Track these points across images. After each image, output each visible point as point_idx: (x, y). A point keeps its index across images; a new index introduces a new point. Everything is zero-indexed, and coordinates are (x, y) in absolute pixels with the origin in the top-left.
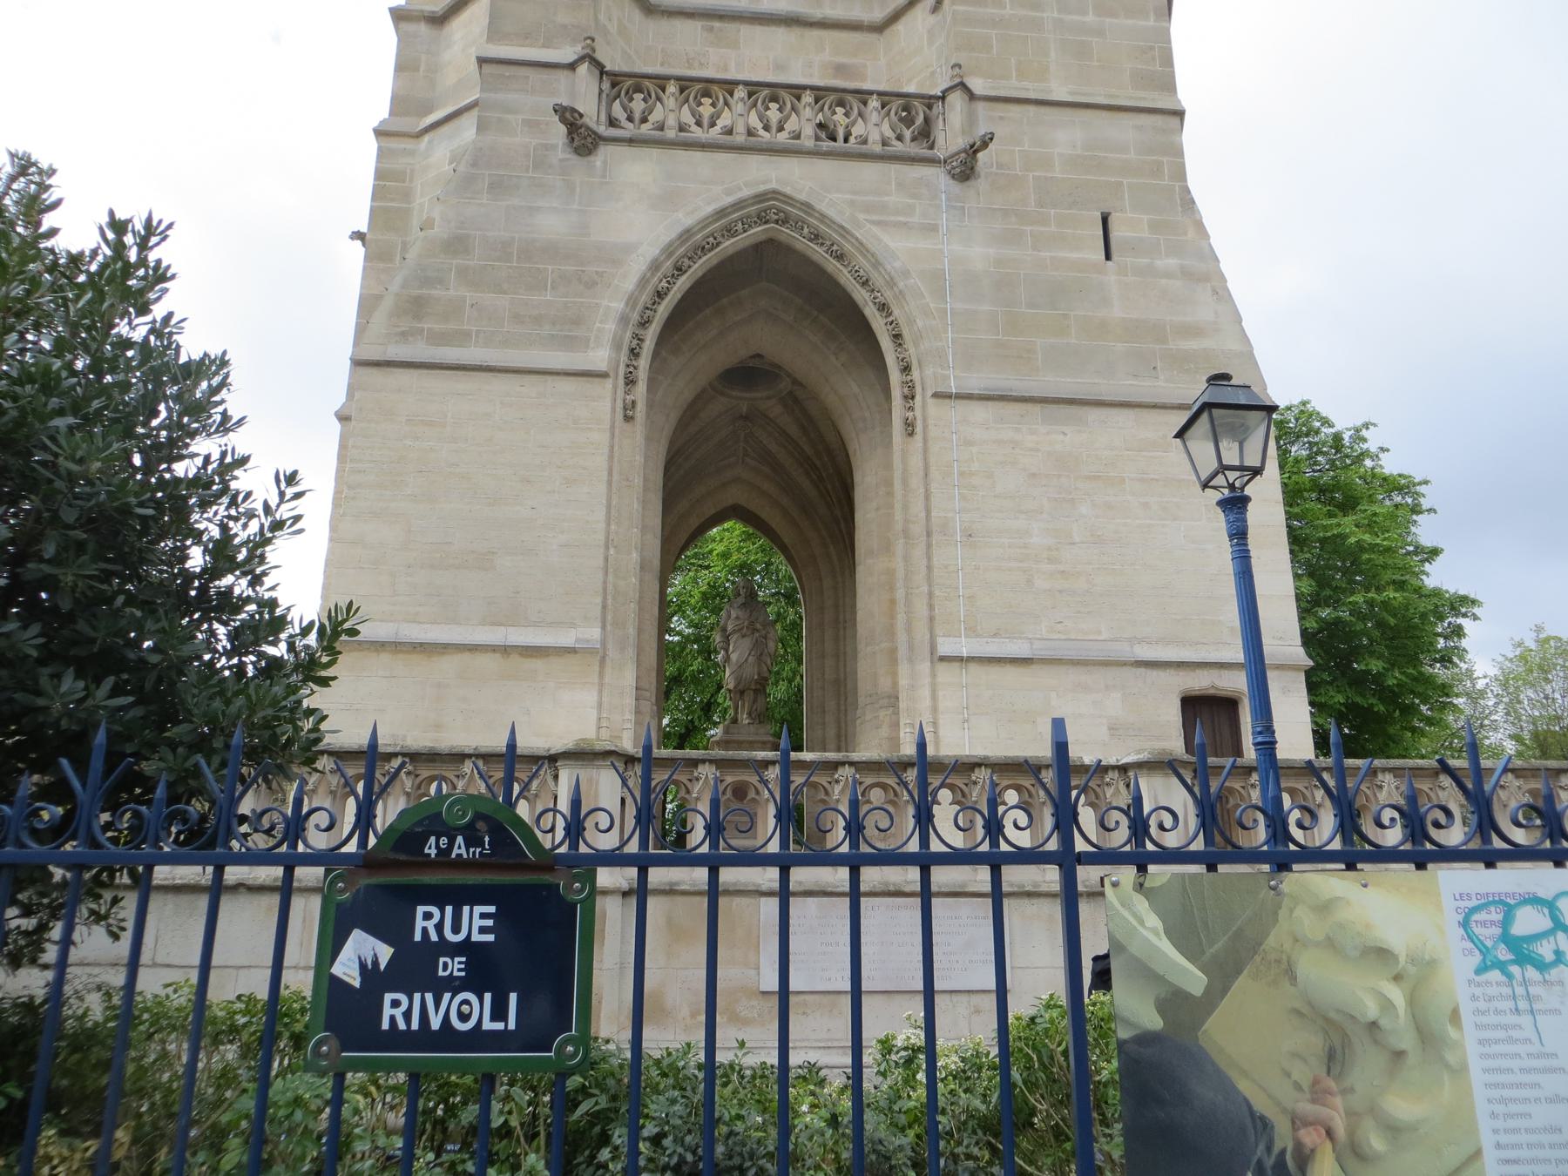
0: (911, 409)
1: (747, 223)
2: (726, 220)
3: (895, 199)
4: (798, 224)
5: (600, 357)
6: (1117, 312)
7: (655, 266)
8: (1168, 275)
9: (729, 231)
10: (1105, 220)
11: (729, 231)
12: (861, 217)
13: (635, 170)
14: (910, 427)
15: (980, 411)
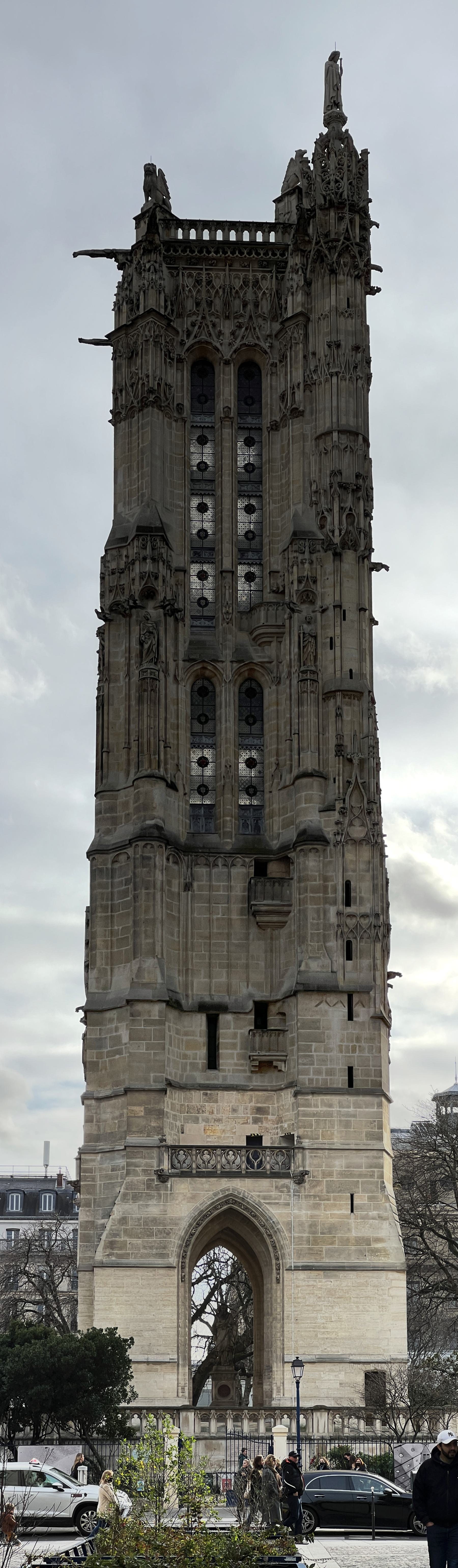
0: (279, 1274)
1: (222, 1205)
2: (214, 1206)
3: (274, 1193)
4: (240, 1205)
5: (173, 1260)
6: (354, 1234)
7: (190, 1225)
8: (374, 1218)
9: (216, 1208)
10: (352, 1196)
11: (216, 1208)
12: (262, 1201)
13: (182, 1187)
14: (278, 1281)
15: (302, 1275)
